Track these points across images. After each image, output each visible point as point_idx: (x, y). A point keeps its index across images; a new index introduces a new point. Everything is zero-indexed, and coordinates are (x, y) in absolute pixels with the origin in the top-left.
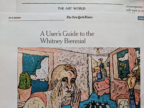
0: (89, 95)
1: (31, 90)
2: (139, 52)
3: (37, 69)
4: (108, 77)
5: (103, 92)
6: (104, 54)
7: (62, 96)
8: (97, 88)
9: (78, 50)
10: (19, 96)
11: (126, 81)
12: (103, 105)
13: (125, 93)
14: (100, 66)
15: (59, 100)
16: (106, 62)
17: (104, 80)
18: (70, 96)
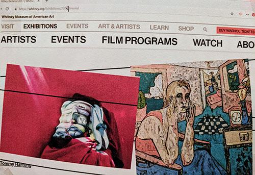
15: (174, 117)
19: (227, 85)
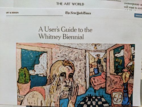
0: (86, 89)
1: (30, 84)
2: (133, 48)
3: (35, 64)
4: (105, 72)
5: (99, 86)
6: (102, 50)
7: (60, 90)
8: (94, 82)
9: (77, 46)
10: (19, 90)
11: (120, 76)
12: (99, 99)
13: (120, 87)
14: (97, 62)
15: (57, 94)
16: (103, 58)
17: (101, 75)
18: (67, 90)
19: (112, 67)
